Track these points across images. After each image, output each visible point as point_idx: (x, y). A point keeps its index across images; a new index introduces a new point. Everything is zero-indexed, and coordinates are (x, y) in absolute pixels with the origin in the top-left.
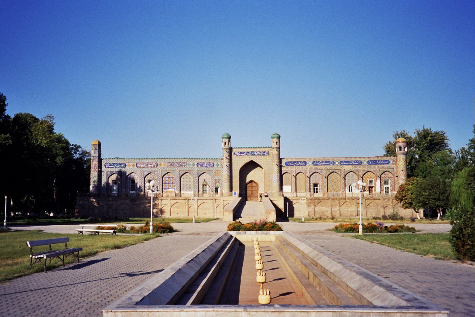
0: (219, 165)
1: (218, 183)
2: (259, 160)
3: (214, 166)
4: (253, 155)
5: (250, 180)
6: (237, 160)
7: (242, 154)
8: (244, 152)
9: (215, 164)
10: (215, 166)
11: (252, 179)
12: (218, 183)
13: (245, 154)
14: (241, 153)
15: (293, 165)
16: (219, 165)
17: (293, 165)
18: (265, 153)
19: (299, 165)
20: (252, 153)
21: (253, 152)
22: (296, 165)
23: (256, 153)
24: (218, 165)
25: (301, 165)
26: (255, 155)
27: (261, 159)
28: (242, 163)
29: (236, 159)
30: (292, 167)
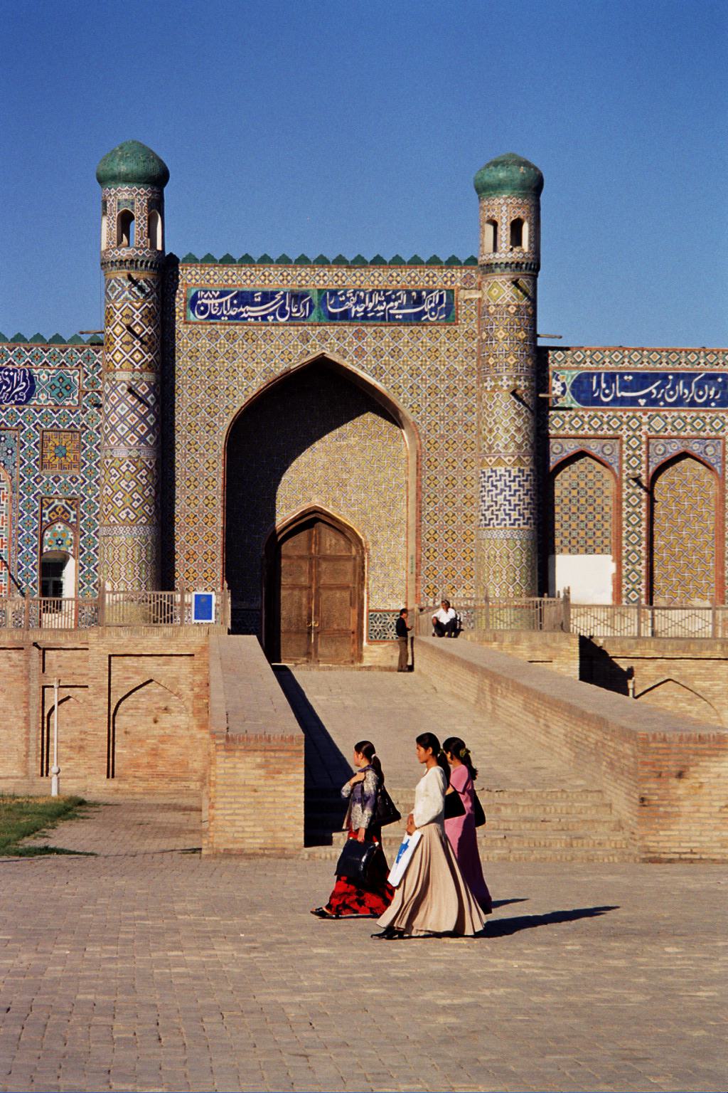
0: (69, 388)
1: (60, 527)
2: (378, 354)
3: (31, 392)
4: (332, 317)
5: (305, 506)
6: (213, 355)
7: (249, 311)
8: (268, 297)
9: (42, 376)
10: (42, 398)
11: (316, 502)
12: (60, 527)
13: (272, 306)
14: (244, 298)
15: (634, 401)
16: (69, 388)
17: (634, 401)
18: (427, 307)
19: (679, 402)
20: (323, 302)
21: (334, 293)
22: (652, 402)
23: (360, 301)
24: (63, 387)
25: (693, 403)
26: (345, 315)
27: (396, 353)
28: (249, 376)
29: (204, 343)
30: (625, 413)
